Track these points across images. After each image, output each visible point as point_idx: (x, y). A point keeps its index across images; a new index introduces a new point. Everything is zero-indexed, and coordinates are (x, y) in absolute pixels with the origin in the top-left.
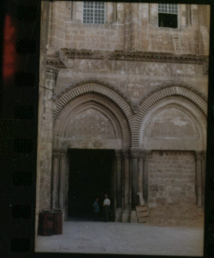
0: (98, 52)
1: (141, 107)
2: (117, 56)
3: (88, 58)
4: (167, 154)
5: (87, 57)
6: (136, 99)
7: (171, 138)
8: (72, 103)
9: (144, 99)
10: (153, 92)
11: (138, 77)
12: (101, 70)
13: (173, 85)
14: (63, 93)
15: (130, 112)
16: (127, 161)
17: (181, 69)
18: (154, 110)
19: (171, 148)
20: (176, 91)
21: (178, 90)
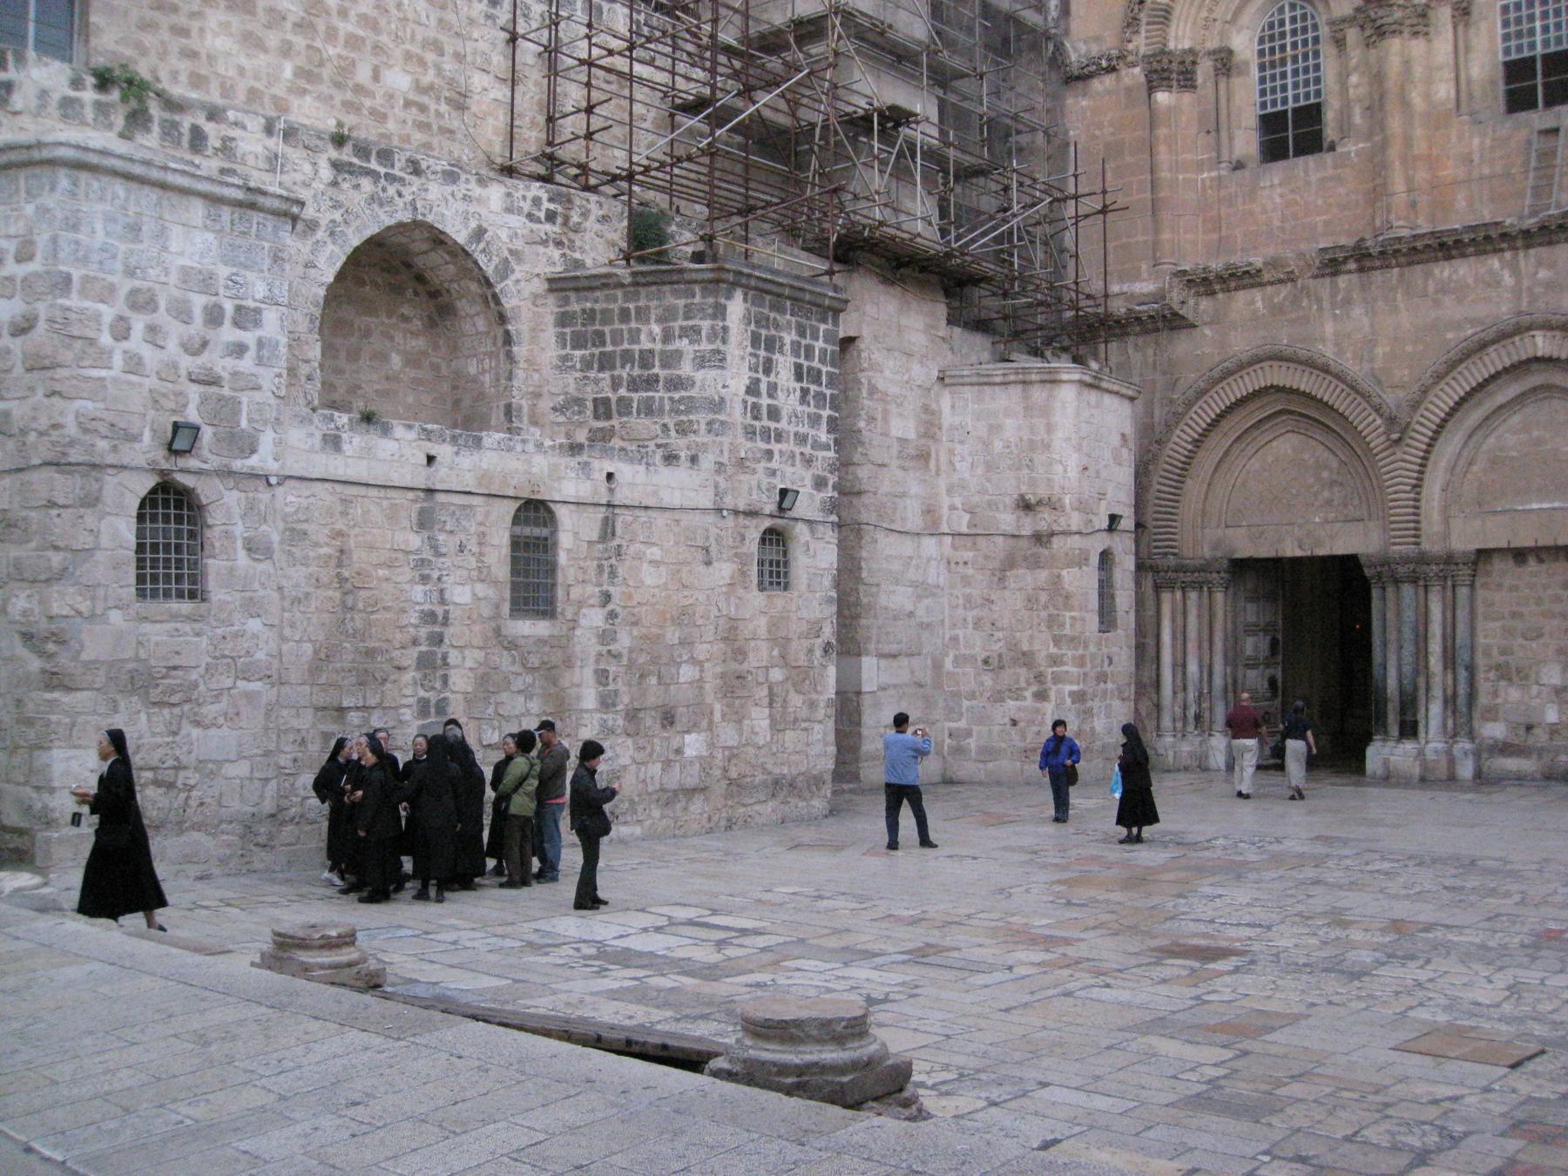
0: (1273, 263)
1: (1417, 417)
2: (1331, 265)
3: (1252, 286)
4: (1541, 561)
5: (1247, 281)
6: (1401, 394)
7: (1545, 506)
8: (1225, 425)
9: (1425, 392)
10: (1452, 365)
11: (1405, 319)
12: (1293, 316)
13: (1519, 330)
14: (1189, 405)
15: (1383, 438)
16: (1390, 590)
17: (1552, 266)
18: (1474, 416)
19: (1549, 542)
20: (1535, 345)
21: (1542, 344)
